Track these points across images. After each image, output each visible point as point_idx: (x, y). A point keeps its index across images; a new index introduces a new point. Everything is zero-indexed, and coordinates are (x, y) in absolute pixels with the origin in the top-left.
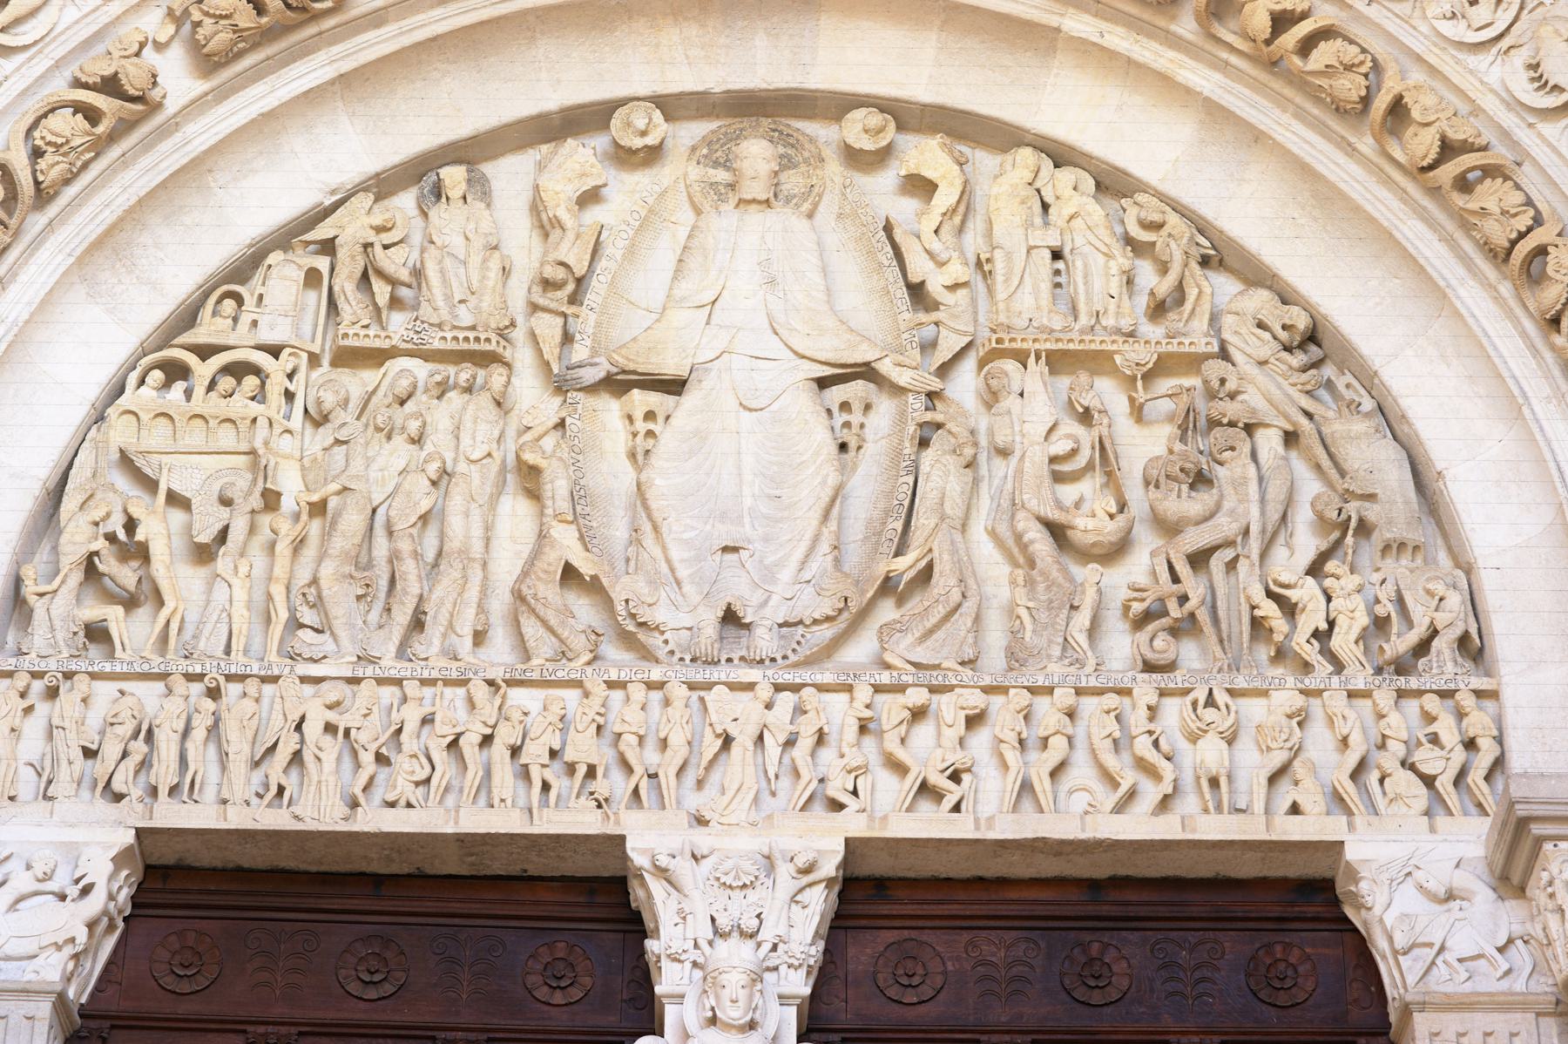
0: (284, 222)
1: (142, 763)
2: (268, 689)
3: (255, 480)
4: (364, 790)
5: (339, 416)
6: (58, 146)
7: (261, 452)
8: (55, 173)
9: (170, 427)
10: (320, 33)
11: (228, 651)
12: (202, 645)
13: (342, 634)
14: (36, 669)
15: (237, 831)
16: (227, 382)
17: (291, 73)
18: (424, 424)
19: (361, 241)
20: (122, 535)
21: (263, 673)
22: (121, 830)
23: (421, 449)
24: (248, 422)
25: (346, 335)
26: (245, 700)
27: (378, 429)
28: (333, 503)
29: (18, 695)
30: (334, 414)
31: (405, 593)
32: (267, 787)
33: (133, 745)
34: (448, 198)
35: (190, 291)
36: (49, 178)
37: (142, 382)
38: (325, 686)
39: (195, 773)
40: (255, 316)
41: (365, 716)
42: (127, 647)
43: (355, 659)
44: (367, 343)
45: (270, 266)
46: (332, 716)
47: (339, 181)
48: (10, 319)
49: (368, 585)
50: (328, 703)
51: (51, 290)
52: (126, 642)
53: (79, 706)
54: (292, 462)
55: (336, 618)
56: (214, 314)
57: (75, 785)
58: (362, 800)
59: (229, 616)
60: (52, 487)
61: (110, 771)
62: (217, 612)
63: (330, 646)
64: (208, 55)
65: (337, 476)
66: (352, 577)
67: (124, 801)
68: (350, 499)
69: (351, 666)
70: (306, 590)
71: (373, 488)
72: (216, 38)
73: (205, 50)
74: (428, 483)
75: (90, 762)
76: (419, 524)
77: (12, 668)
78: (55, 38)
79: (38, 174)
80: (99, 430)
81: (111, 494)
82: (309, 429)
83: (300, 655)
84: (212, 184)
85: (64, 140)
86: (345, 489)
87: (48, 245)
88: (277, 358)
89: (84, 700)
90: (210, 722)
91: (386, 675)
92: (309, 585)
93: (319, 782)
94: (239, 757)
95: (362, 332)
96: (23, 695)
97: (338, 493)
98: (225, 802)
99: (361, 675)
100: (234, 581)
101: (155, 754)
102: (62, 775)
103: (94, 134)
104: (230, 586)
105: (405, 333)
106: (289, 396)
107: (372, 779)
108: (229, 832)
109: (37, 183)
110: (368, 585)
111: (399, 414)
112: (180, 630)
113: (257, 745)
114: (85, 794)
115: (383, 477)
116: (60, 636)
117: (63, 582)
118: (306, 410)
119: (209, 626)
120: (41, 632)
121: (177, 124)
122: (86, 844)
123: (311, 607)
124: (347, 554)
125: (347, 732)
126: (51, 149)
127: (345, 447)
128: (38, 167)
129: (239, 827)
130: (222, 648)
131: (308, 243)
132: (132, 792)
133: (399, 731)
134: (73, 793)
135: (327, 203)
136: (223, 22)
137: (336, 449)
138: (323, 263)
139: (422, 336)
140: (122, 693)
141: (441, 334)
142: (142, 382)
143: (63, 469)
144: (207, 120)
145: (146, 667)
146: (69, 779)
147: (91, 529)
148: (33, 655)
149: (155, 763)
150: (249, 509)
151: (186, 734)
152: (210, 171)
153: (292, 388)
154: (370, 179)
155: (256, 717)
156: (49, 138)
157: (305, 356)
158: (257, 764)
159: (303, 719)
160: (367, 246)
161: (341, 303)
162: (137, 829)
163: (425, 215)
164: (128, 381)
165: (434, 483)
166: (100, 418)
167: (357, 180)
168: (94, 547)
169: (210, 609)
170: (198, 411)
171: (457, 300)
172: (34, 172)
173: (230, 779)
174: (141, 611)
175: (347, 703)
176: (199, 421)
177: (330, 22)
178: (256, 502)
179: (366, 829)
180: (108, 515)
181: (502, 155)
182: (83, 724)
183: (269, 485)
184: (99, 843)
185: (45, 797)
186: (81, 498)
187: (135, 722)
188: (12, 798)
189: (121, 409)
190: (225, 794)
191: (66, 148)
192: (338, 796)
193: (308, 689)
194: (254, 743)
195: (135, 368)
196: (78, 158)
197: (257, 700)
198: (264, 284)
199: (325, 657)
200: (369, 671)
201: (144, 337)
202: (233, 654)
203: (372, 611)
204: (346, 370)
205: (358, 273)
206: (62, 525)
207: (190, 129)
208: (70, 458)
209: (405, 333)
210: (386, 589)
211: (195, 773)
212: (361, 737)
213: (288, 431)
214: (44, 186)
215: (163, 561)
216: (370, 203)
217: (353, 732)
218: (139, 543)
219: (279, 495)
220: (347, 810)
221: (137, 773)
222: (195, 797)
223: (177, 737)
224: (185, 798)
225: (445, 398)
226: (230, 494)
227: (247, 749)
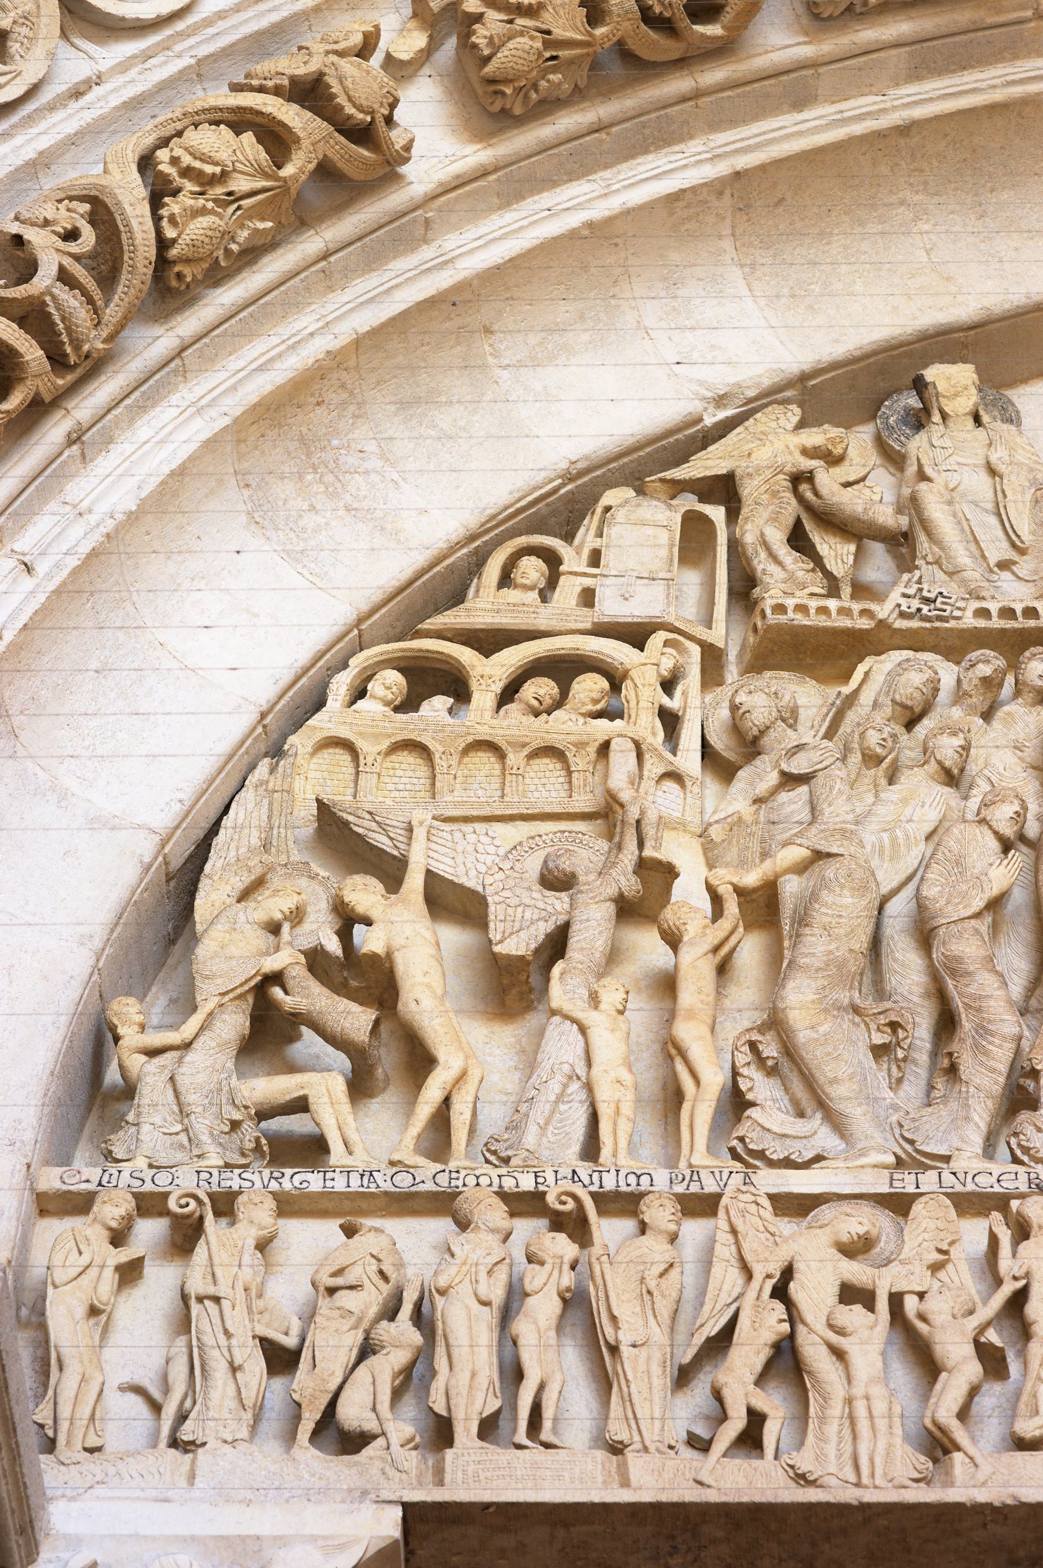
0: (630, 441)
1: (407, 1372)
2: (694, 1230)
3: (620, 847)
4: (963, 1414)
5: (781, 738)
6: (207, 182)
7: (625, 796)
8: (198, 228)
9: (423, 771)
10: (697, 95)
11: (591, 1149)
12: (530, 1138)
13: (856, 1113)
14: (148, 1187)
15: (657, 1507)
16: (541, 688)
17: (641, 169)
18: (966, 748)
19: (788, 468)
20: (333, 945)
21: (680, 1189)
22: (368, 1510)
23: (966, 798)
24: (592, 749)
25: (780, 609)
26: (646, 1240)
27: (872, 759)
28: (791, 887)
29: (105, 1234)
30: (772, 734)
31: (983, 1030)
32: (723, 1417)
33: (386, 1330)
34: (944, 416)
35: (454, 538)
36: (185, 239)
37: (360, 693)
38: (825, 1212)
39: (542, 1387)
40: (588, 582)
41: (935, 1268)
42: (358, 1150)
43: (891, 1159)
44: (822, 621)
45: (608, 509)
46: (857, 1271)
47: (732, 380)
48: (93, 519)
49: (894, 1026)
50: (845, 1238)
51: (180, 473)
52: (353, 1137)
53: (250, 1257)
54: (685, 839)
55: (835, 1081)
56: (506, 580)
57: (248, 1416)
58: (960, 1434)
59: (589, 1087)
60: (176, 863)
61: (333, 1386)
62: (559, 1078)
63: (826, 1139)
64: (492, 81)
65: (800, 834)
66: (856, 1010)
67: (368, 1451)
68: (830, 870)
69: (886, 1173)
70: (755, 1037)
71: (875, 863)
72: (511, 45)
73: (489, 69)
74: (994, 845)
75: (278, 1383)
76: (988, 919)
77: (91, 1187)
78: (194, 29)
79: (165, 223)
80: (273, 770)
81: (304, 882)
82: (712, 786)
83: (760, 1155)
84: (490, 360)
85: (218, 170)
86: (819, 856)
87: (175, 399)
88: (640, 645)
89: (263, 1246)
90: (568, 1279)
91: (970, 1187)
92: (762, 1029)
93: (849, 1401)
94: (643, 1352)
95: (813, 604)
96: (118, 1238)
97: (801, 868)
98: (617, 1449)
99: (911, 1189)
100: (589, 1017)
101: (440, 1350)
102: (215, 1395)
103: (277, 179)
104: (583, 1030)
105: (904, 603)
106: (670, 721)
107: (974, 1391)
108: (636, 1511)
109: (163, 244)
110: (894, 1026)
111: (909, 745)
112: (472, 1131)
113: (680, 1338)
114: (273, 1447)
115: (894, 841)
116: (203, 1124)
117: (202, 1029)
118: (705, 744)
119: (539, 1113)
120: (158, 1120)
121: (427, 222)
122: (282, 1541)
123: (772, 1072)
124: (840, 967)
125: (896, 1300)
126: (189, 186)
127: (804, 789)
128: (164, 212)
129: (664, 1498)
130: (576, 1148)
131: (678, 487)
132: (390, 1427)
133: (1019, 1299)
134: (244, 1433)
135: (709, 421)
136: (521, 21)
137: (784, 796)
138: (717, 513)
139: (938, 605)
140: (350, 1231)
141: (976, 605)
142: (360, 693)
143: (200, 834)
144: (483, 230)
145: (404, 1181)
146: (233, 1404)
147: (261, 939)
148: (141, 1163)
149: (441, 1363)
150: (612, 891)
151: (507, 1315)
152: (488, 331)
153: (673, 704)
154: (789, 385)
155: (674, 1273)
156: (187, 160)
157: (695, 650)
158: (683, 1377)
159: (788, 1273)
160: (799, 479)
161: (761, 563)
162: (408, 1508)
163: (894, 459)
164: (333, 686)
165: (1006, 846)
166: (277, 752)
167: (766, 382)
168: (271, 964)
169: (543, 1072)
170: (484, 732)
171: (992, 562)
172: (157, 219)
173: (628, 1400)
174: (375, 1105)
175: (885, 1245)
176: (484, 761)
177: (714, 75)
178: (625, 880)
179: (982, 1496)
180: (297, 916)
181: (1025, 381)
182: (260, 1296)
183: (648, 852)
184: (313, 1539)
185: (174, 1443)
186: (239, 882)
187: (386, 1289)
188: (91, 1451)
189: (319, 736)
190: (618, 1431)
191: (219, 191)
192: (898, 1431)
193: (785, 1226)
194: (672, 1329)
195: (345, 665)
196: (242, 226)
197: (673, 1238)
198: (600, 534)
199: (818, 1158)
200: (929, 1180)
201: (365, 607)
202: (606, 1153)
203: (906, 1086)
204: (785, 674)
205: (790, 521)
206: (199, 928)
207: (451, 242)
208: (213, 817)
209: (904, 603)
210: (928, 1046)
211: (542, 1387)
212: (939, 1307)
213: (674, 776)
214: (174, 252)
215: (428, 986)
216: (795, 420)
217: (911, 1304)
218: (374, 957)
219: (669, 872)
220: (924, 1463)
221: (397, 1394)
222: (545, 1435)
223: (488, 1318)
224: (521, 1437)
225: (1000, 714)
226: (566, 864)
227: (658, 1335)
